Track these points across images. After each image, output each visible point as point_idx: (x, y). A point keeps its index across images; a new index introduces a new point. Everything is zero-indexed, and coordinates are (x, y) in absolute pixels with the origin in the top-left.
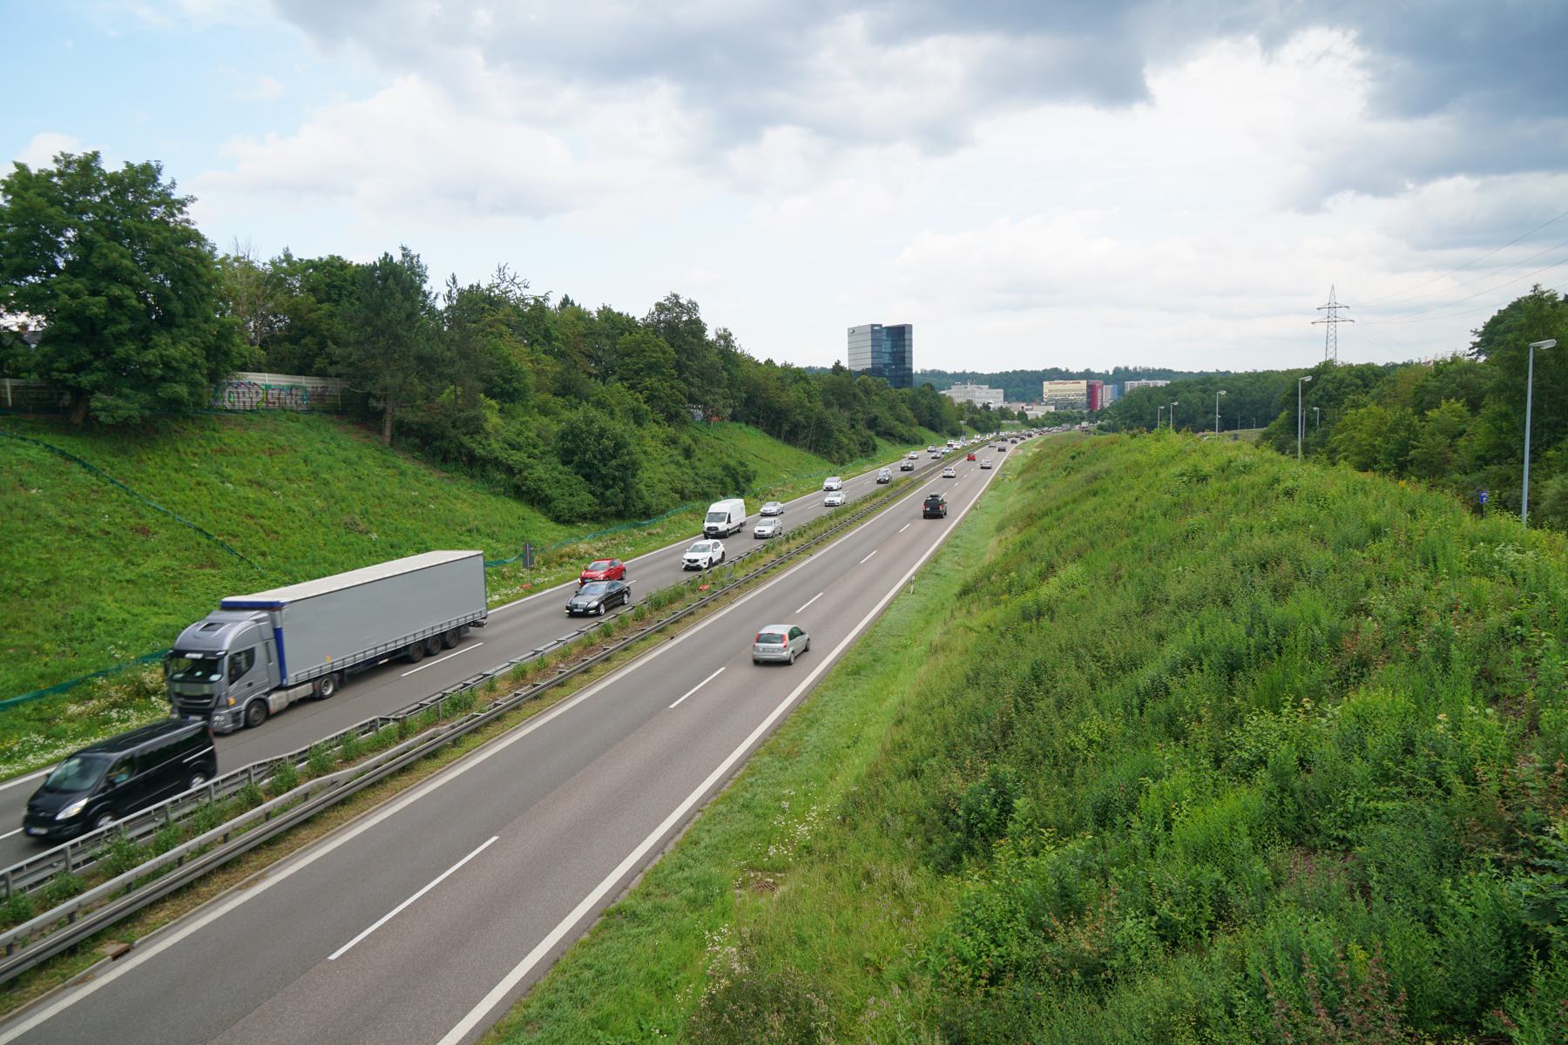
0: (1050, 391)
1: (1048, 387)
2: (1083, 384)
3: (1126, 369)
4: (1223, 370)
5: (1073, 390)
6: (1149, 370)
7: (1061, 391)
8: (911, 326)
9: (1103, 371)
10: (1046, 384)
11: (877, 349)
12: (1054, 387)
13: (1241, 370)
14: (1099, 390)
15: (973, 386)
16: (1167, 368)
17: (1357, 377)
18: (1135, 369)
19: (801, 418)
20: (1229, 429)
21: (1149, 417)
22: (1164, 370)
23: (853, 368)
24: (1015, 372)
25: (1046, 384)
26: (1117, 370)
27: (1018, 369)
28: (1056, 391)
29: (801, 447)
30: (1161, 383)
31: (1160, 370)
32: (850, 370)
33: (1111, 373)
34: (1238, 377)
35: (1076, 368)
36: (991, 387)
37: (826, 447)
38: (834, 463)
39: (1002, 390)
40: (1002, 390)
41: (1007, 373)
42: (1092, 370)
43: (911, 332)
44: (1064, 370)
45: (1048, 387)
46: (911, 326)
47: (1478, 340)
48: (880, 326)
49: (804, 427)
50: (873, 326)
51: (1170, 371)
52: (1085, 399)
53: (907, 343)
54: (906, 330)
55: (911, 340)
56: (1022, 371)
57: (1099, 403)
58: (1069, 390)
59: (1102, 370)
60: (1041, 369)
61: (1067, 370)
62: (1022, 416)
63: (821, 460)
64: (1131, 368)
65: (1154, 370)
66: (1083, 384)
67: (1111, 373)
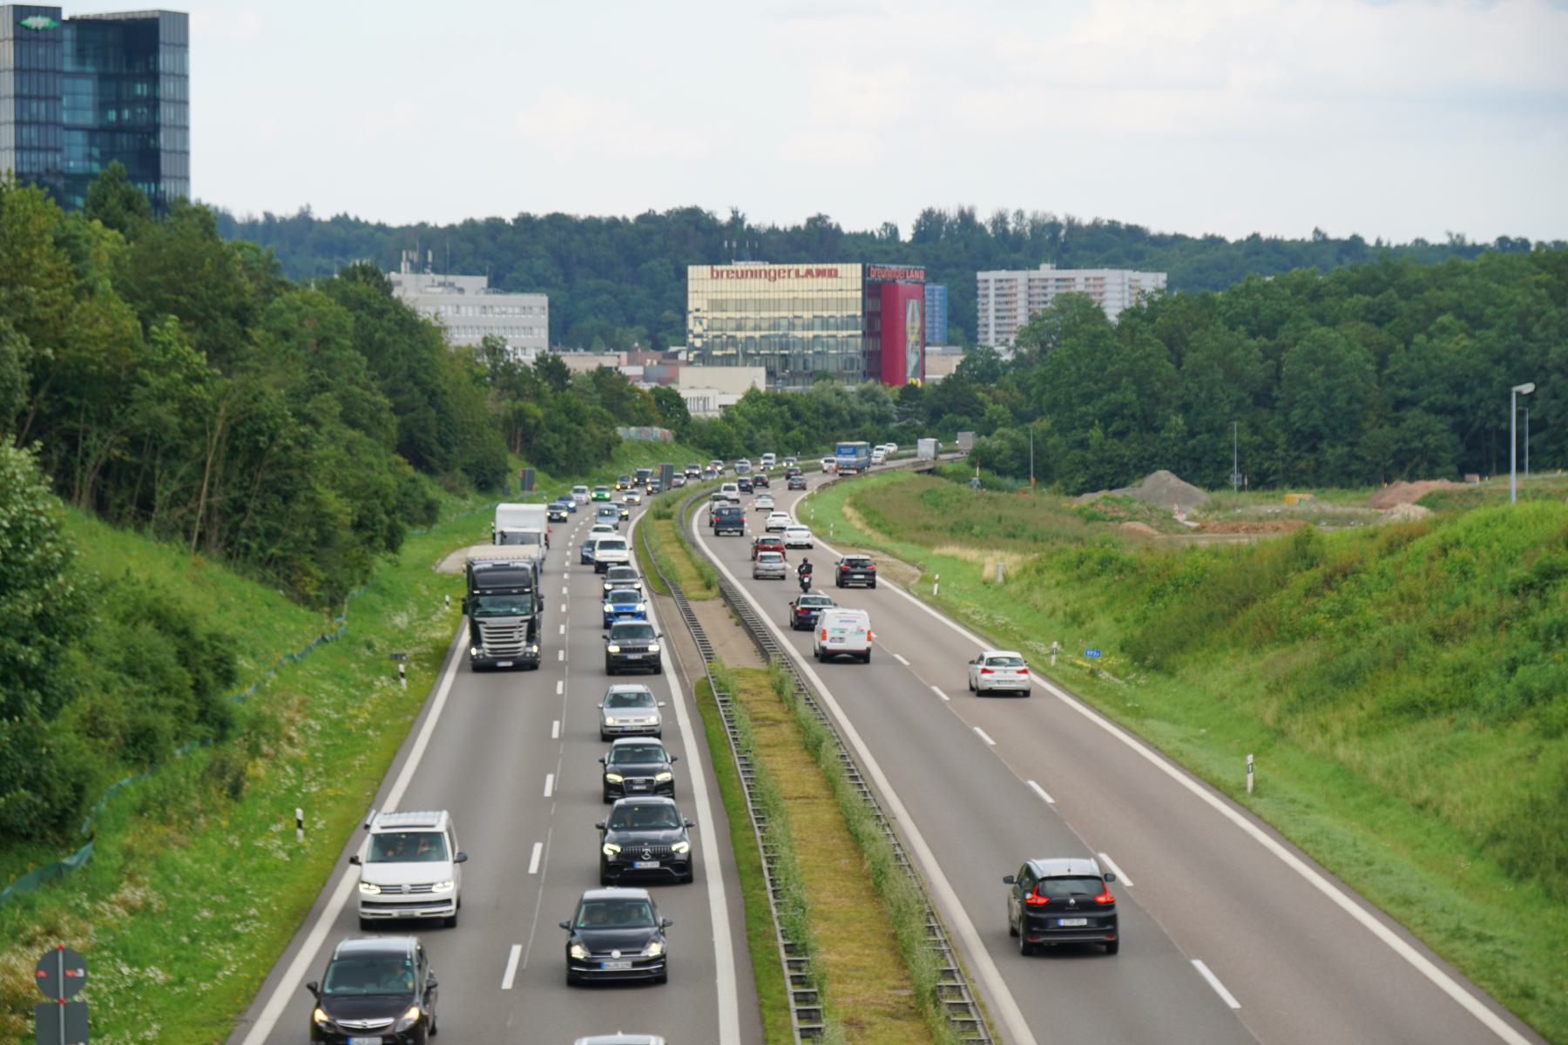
0: (716, 305)
1: (703, 284)
2: (850, 276)
3: (966, 219)
4: (1339, 231)
5: (808, 304)
6: (1054, 226)
7: (760, 305)
8: (181, 20)
10: (698, 274)
11: (39, 109)
14: (912, 307)
18: (1000, 221)
19: (166, 413)
21: (1178, 421)
22: (1113, 227)
24: (525, 221)
25: (698, 274)
26: (930, 224)
27: (540, 210)
28: (740, 305)
29: (166, 533)
31: (1096, 227)
33: (906, 235)
36: (499, 283)
37: (272, 535)
38: (305, 600)
39: (540, 301)
40: (540, 301)
42: (833, 220)
43: (183, 46)
44: (724, 217)
45: (703, 284)
46: (181, 20)
48: (54, 12)
49: (174, 452)
50: (21, 12)
51: (1135, 232)
53: (167, 88)
54: (164, 35)
55: (183, 77)
60: (628, 208)
61: (737, 220)
62: (669, 405)
64: (983, 217)
65: (1073, 227)
66: (850, 276)
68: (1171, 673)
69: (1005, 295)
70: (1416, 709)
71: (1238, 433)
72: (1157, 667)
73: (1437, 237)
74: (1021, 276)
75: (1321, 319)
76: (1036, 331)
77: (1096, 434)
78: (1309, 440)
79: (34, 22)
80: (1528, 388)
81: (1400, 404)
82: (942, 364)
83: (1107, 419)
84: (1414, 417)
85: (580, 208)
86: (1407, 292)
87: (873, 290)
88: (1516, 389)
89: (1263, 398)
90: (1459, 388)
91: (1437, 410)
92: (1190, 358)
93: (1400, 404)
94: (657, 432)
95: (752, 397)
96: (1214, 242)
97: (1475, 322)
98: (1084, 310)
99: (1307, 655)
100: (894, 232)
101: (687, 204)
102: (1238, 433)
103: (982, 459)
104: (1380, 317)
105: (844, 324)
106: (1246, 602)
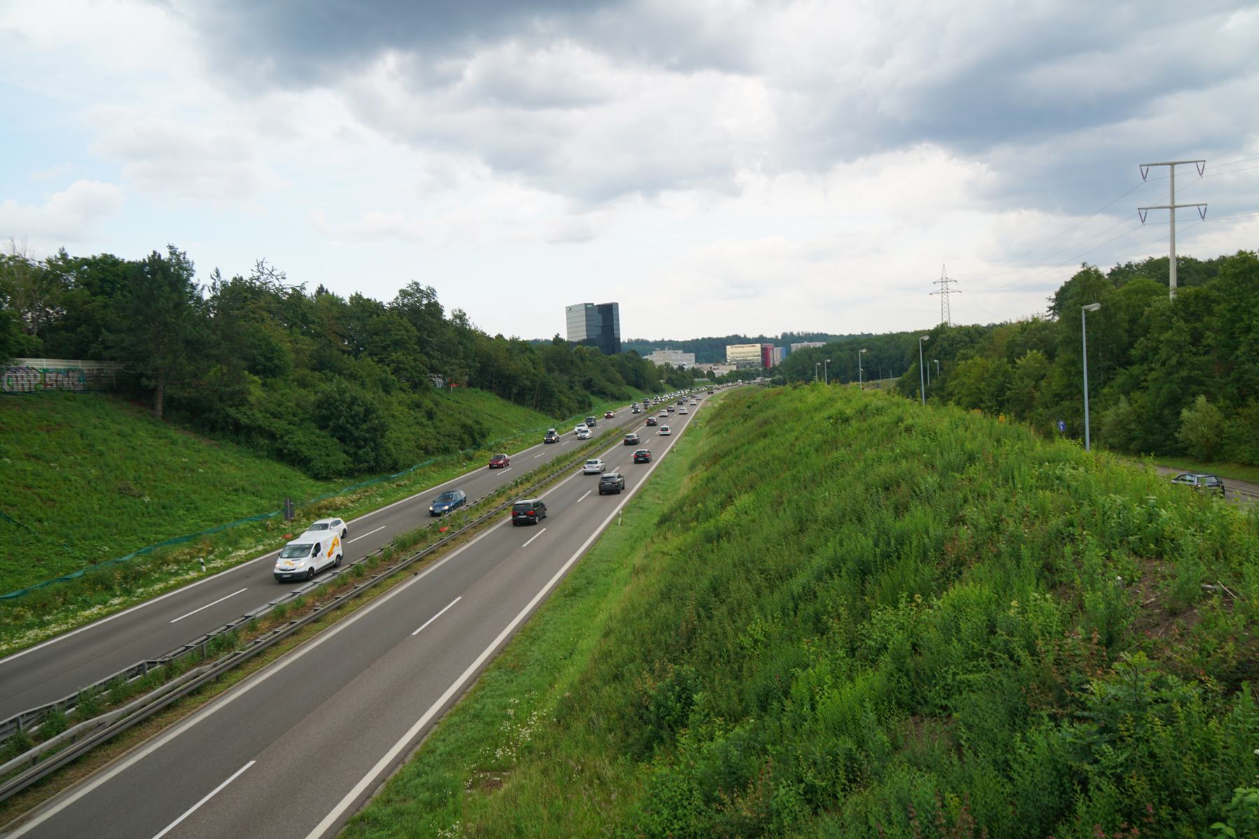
0: (732, 353)
2: (758, 346)
3: (792, 334)
4: (866, 332)
5: (750, 352)
7: (740, 353)
8: (617, 304)
9: (773, 336)
10: (728, 347)
13: (880, 332)
14: (771, 352)
15: (670, 351)
16: (823, 332)
17: (965, 335)
18: (799, 334)
20: (873, 379)
23: (570, 340)
24: (703, 339)
25: (728, 347)
26: (784, 335)
27: (706, 337)
30: (819, 344)
31: (818, 334)
32: (568, 342)
33: (780, 338)
34: (878, 338)
35: (752, 334)
39: (693, 354)
40: (693, 354)
41: (697, 340)
42: (765, 335)
43: (618, 309)
44: (742, 336)
46: (617, 304)
48: (592, 304)
50: (586, 304)
51: (826, 335)
52: (759, 359)
56: (710, 338)
57: (771, 362)
58: (747, 352)
59: (773, 336)
62: (711, 374)
63: (545, 417)
64: (795, 333)
66: (758, 346)
67: (780, 338)
79: (588, 306)
85: (715, 336)
87: (762, 349)
101: (735, 334)
103: (773, 382)
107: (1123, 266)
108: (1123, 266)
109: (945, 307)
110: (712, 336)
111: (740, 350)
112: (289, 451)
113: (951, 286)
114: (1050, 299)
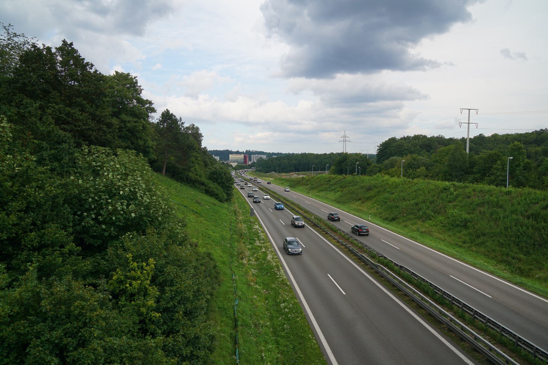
0: (232, 158)
1: (231, 156)
2: (243, 155)
3: (250, 151)
6: (257, 151)
7: (235, 158)
9: (242, 151)
12: (233, 156)
13: (284, 153)
16: (262, 151)
17: (360, 158)
18: (252, 151)
24: (214, 150)
27: (215, 150)
33: (245, 152)
39: (219, 157)
40: (219, 157)
41: (211, 151)
44: (230, 150)
45: (231, 156)
47: (379, 148)
51: (263, 152)
56: (216, 150)
61: (231, 151)
63: (172, 181)
64: (251, 151)
65: (258, 152)
66: (243, 155)
67: (245, 152)
68: (295, 188)
69: (253, 157)
70: (322, 191)
71: (277, 168)
72: (293, 187)
73: (287, 153)
74: (255, 155)
75: (283, 159)
76: (258, 160)
77: (266, 168)
78: (283, 169)
80: (358, 163)
81: (290, 166)
82: (250, 163)
83: (267, 167)
84: (291, 167)
86: (290, 157)
87: (244, 156)
88: (509, 158)
89: (279, 166)
90: (295, 165)
91: (293, 167)
92: (274, 162)
93: (290, 166)
94: (231, 168)
95: (237, 165)
96: (269, 153)
97: (296, 160)
98: (261, 158)
99: (309, 186)
100: (244, 152)
102: (277, 168)
103: (256, 170)
104: (288, 159)
105: (242, 159)
106: (300, 182)
107: (406, 137)
108: (406, 137)
109: (345, 147)
110: (318, 153)
111: (235, 156)
112: (211, 191)
113: (347, 139)
114: (378, 146)
